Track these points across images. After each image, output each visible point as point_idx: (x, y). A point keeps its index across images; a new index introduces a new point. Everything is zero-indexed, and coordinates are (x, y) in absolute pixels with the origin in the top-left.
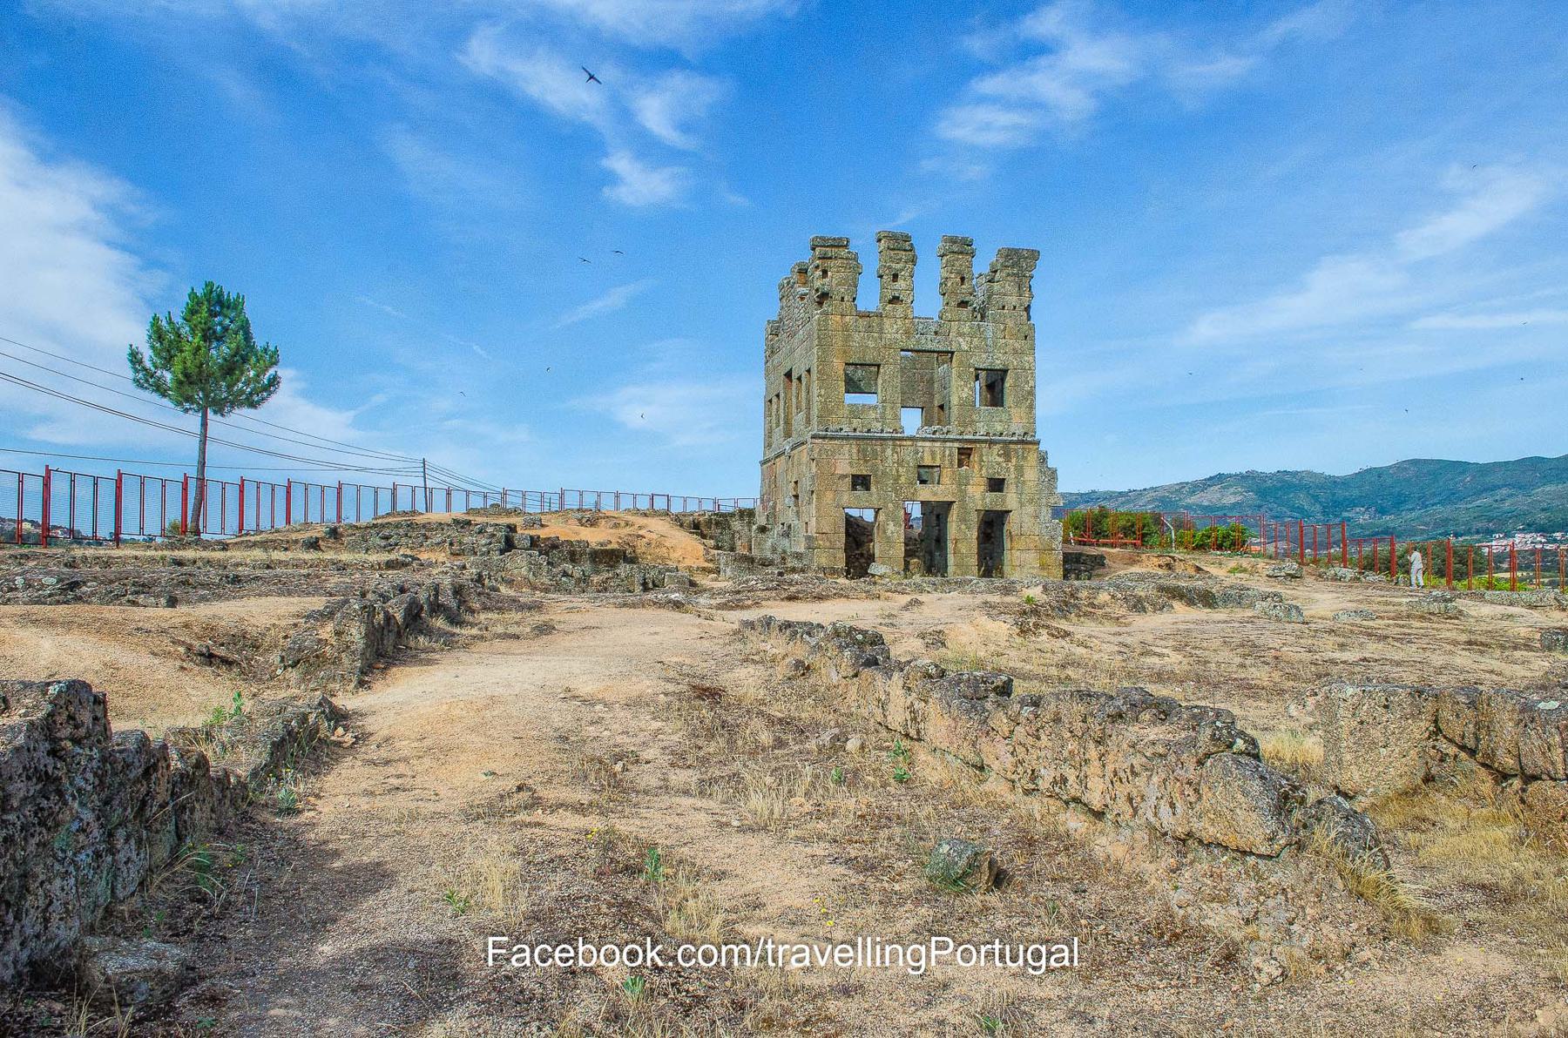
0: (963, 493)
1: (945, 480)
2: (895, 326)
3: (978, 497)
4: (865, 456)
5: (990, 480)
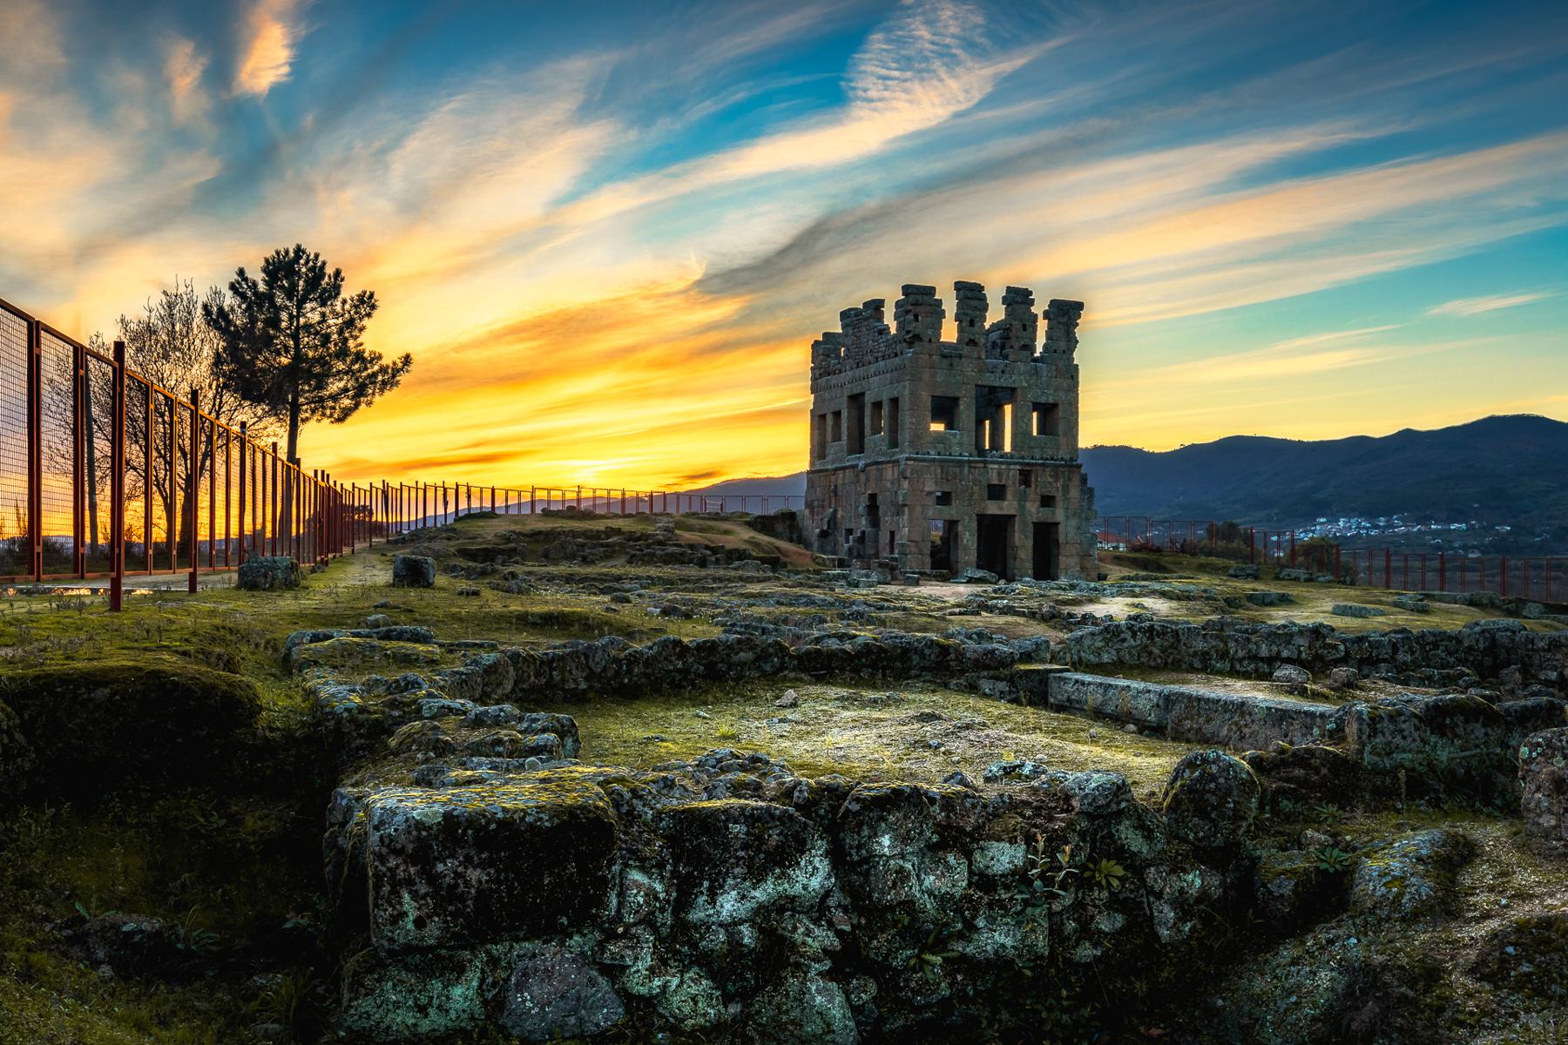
0: (1022, 507)
1: (1009, 496)
3: (1033, 510)
5: (1042, 497)
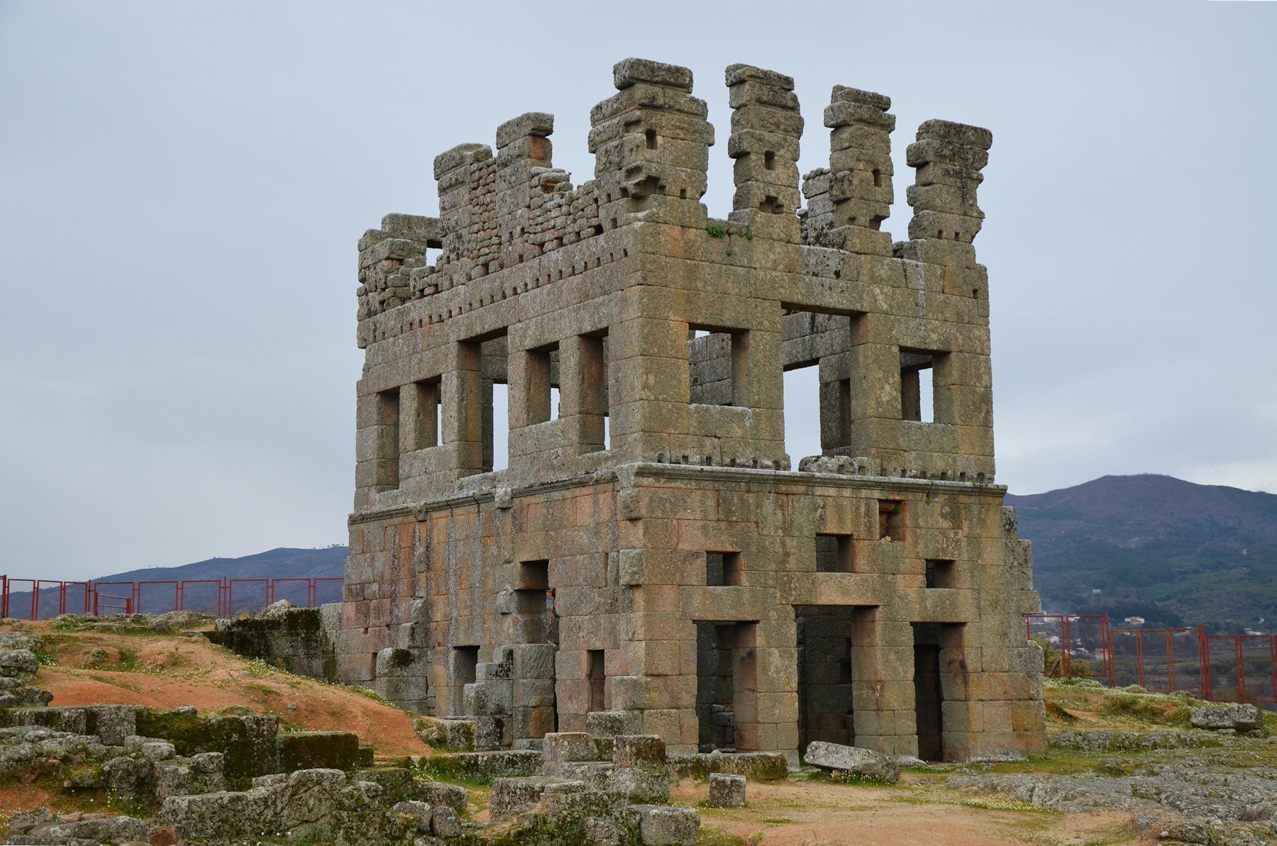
2: (772, 256)
4: (729, 513)
